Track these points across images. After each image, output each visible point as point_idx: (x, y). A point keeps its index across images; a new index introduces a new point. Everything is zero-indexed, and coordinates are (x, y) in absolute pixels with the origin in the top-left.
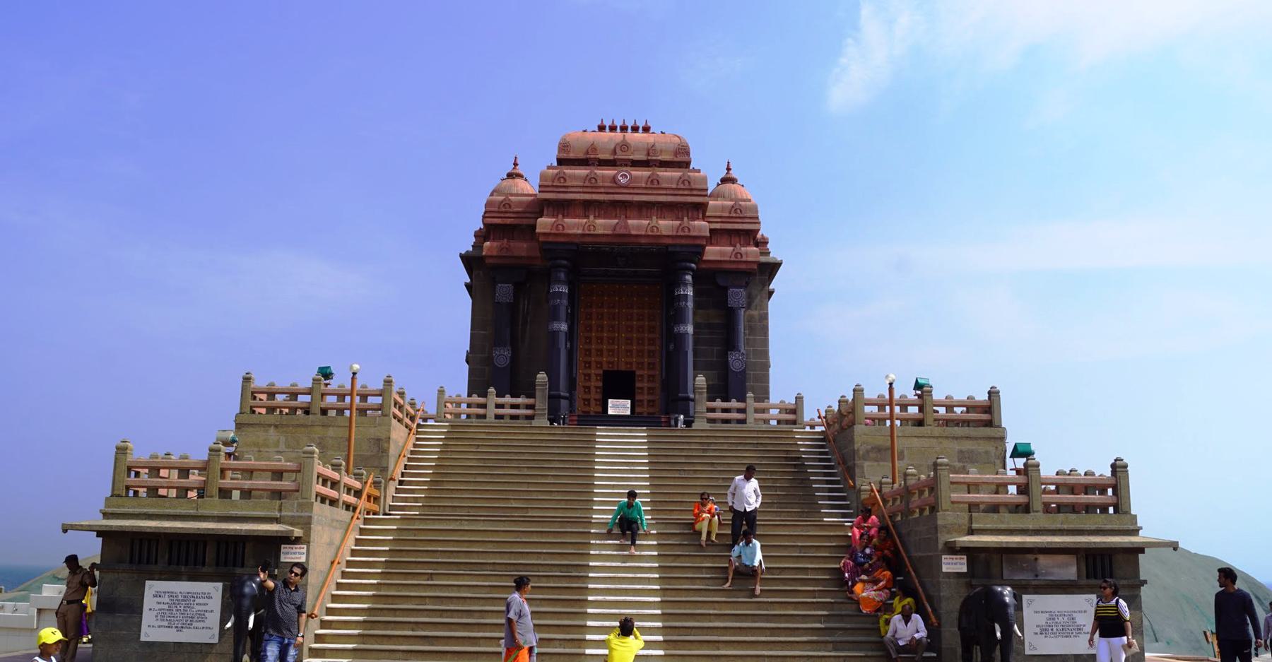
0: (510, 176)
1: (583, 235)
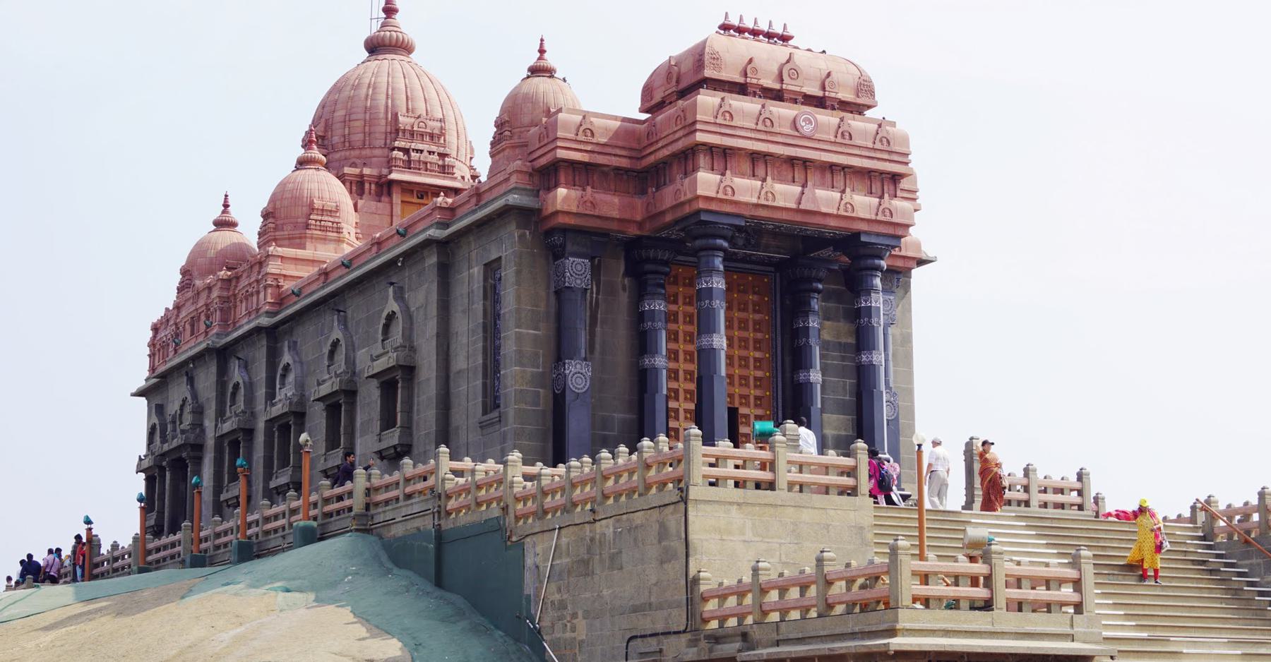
0: (535, 71)
1: (757, 206)
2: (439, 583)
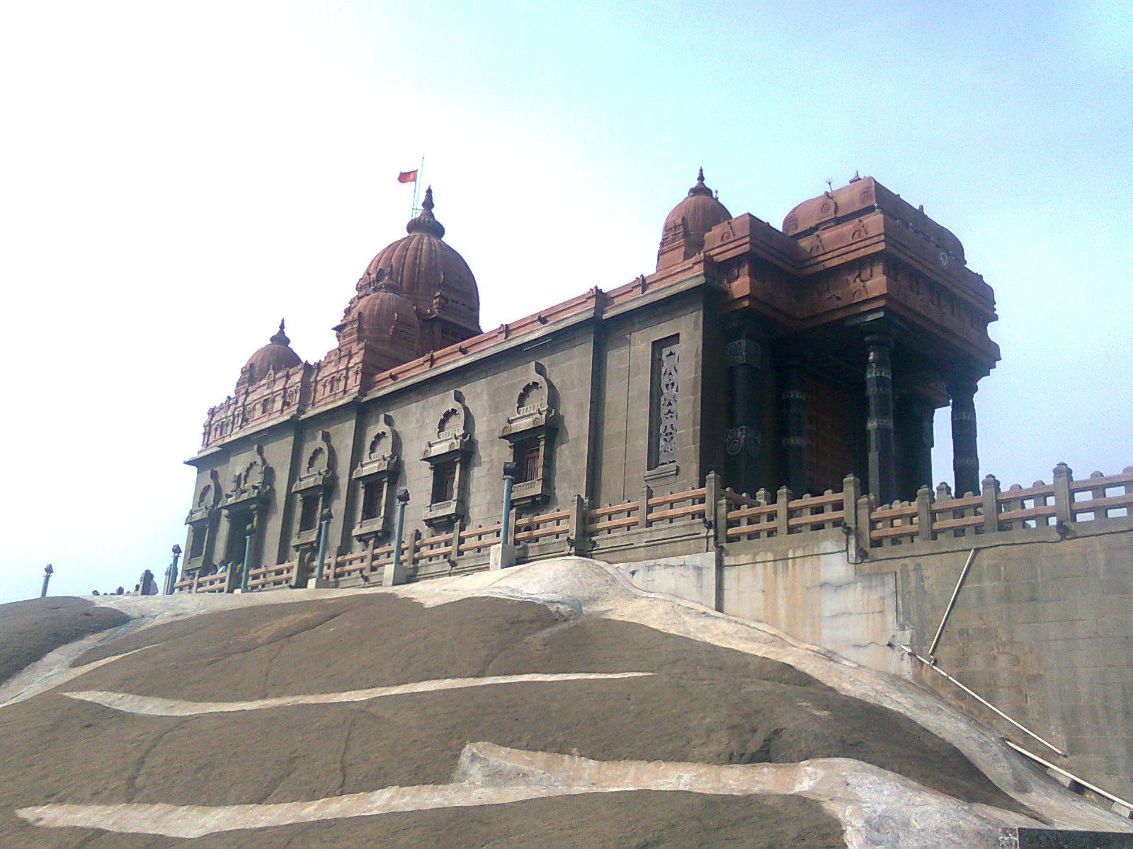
0: (694, 191)
1: (919, 315)
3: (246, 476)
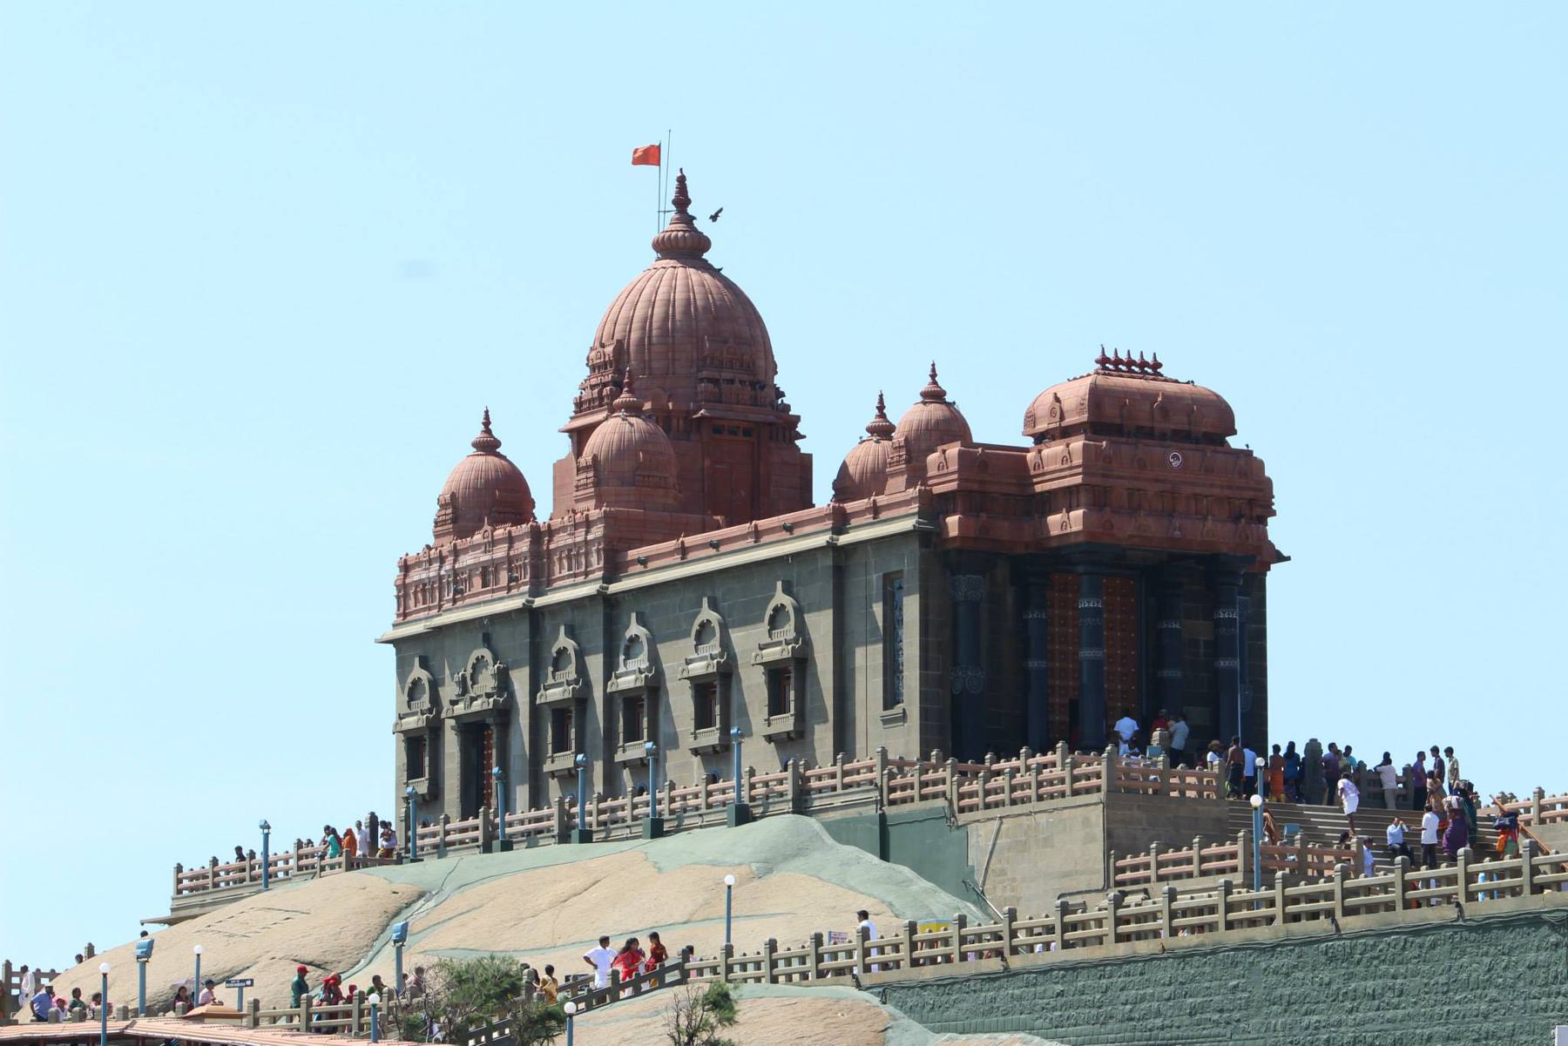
2: (884, 856)
3: (472, 676)
